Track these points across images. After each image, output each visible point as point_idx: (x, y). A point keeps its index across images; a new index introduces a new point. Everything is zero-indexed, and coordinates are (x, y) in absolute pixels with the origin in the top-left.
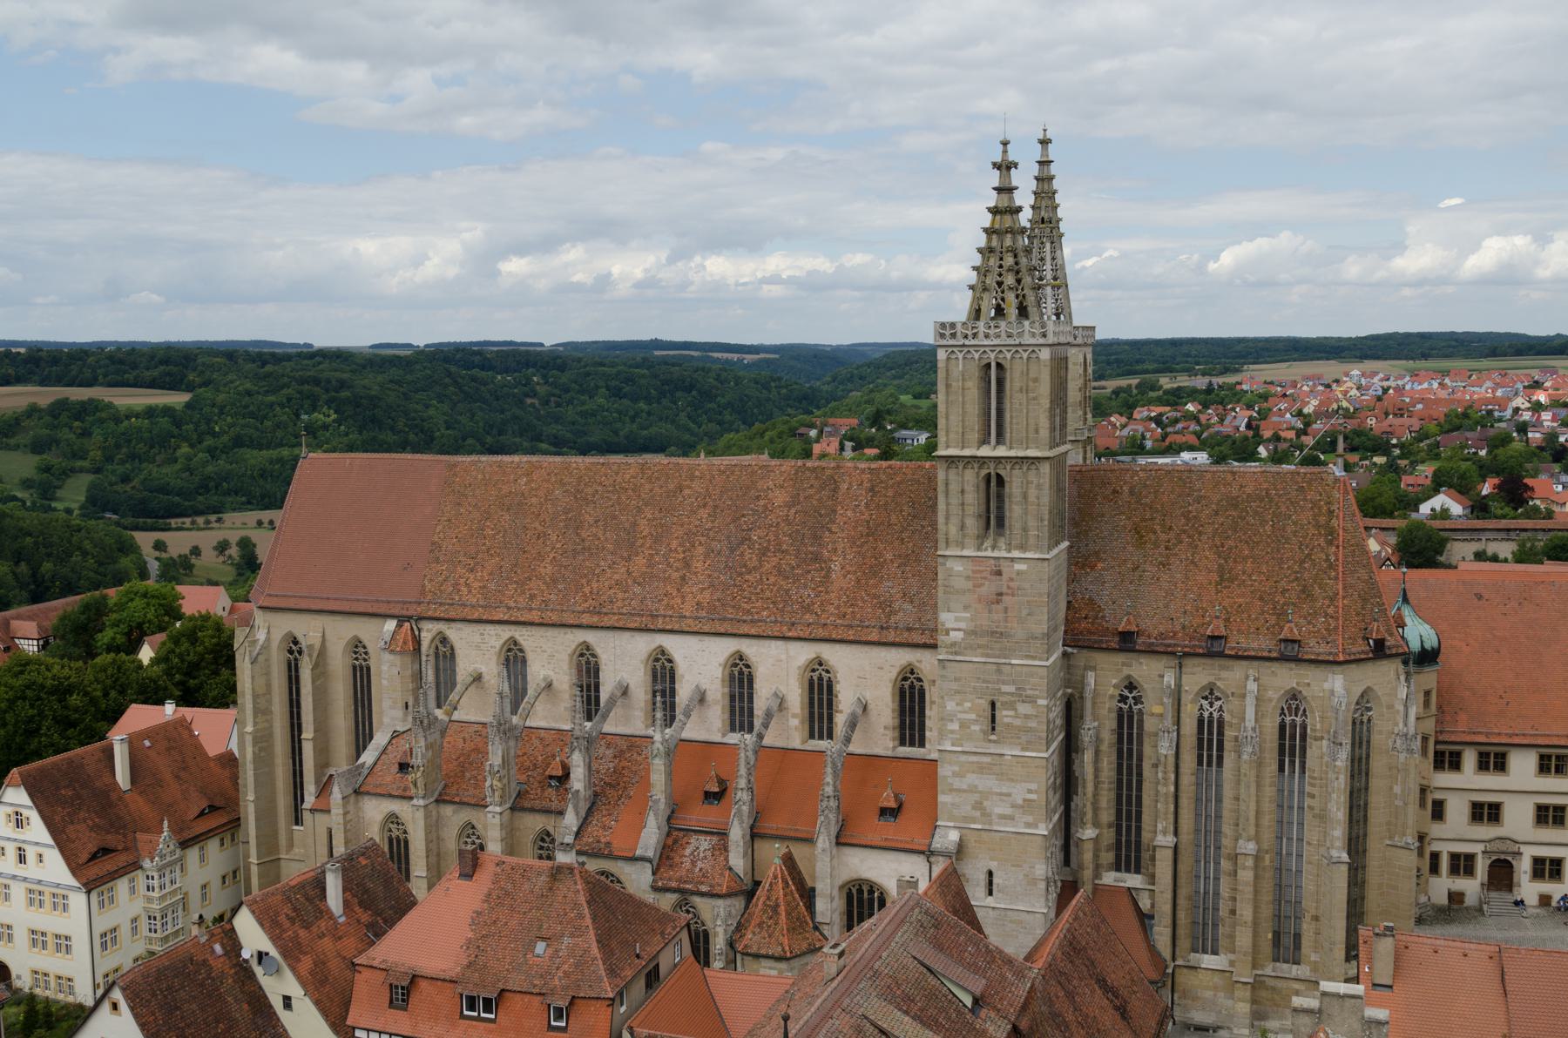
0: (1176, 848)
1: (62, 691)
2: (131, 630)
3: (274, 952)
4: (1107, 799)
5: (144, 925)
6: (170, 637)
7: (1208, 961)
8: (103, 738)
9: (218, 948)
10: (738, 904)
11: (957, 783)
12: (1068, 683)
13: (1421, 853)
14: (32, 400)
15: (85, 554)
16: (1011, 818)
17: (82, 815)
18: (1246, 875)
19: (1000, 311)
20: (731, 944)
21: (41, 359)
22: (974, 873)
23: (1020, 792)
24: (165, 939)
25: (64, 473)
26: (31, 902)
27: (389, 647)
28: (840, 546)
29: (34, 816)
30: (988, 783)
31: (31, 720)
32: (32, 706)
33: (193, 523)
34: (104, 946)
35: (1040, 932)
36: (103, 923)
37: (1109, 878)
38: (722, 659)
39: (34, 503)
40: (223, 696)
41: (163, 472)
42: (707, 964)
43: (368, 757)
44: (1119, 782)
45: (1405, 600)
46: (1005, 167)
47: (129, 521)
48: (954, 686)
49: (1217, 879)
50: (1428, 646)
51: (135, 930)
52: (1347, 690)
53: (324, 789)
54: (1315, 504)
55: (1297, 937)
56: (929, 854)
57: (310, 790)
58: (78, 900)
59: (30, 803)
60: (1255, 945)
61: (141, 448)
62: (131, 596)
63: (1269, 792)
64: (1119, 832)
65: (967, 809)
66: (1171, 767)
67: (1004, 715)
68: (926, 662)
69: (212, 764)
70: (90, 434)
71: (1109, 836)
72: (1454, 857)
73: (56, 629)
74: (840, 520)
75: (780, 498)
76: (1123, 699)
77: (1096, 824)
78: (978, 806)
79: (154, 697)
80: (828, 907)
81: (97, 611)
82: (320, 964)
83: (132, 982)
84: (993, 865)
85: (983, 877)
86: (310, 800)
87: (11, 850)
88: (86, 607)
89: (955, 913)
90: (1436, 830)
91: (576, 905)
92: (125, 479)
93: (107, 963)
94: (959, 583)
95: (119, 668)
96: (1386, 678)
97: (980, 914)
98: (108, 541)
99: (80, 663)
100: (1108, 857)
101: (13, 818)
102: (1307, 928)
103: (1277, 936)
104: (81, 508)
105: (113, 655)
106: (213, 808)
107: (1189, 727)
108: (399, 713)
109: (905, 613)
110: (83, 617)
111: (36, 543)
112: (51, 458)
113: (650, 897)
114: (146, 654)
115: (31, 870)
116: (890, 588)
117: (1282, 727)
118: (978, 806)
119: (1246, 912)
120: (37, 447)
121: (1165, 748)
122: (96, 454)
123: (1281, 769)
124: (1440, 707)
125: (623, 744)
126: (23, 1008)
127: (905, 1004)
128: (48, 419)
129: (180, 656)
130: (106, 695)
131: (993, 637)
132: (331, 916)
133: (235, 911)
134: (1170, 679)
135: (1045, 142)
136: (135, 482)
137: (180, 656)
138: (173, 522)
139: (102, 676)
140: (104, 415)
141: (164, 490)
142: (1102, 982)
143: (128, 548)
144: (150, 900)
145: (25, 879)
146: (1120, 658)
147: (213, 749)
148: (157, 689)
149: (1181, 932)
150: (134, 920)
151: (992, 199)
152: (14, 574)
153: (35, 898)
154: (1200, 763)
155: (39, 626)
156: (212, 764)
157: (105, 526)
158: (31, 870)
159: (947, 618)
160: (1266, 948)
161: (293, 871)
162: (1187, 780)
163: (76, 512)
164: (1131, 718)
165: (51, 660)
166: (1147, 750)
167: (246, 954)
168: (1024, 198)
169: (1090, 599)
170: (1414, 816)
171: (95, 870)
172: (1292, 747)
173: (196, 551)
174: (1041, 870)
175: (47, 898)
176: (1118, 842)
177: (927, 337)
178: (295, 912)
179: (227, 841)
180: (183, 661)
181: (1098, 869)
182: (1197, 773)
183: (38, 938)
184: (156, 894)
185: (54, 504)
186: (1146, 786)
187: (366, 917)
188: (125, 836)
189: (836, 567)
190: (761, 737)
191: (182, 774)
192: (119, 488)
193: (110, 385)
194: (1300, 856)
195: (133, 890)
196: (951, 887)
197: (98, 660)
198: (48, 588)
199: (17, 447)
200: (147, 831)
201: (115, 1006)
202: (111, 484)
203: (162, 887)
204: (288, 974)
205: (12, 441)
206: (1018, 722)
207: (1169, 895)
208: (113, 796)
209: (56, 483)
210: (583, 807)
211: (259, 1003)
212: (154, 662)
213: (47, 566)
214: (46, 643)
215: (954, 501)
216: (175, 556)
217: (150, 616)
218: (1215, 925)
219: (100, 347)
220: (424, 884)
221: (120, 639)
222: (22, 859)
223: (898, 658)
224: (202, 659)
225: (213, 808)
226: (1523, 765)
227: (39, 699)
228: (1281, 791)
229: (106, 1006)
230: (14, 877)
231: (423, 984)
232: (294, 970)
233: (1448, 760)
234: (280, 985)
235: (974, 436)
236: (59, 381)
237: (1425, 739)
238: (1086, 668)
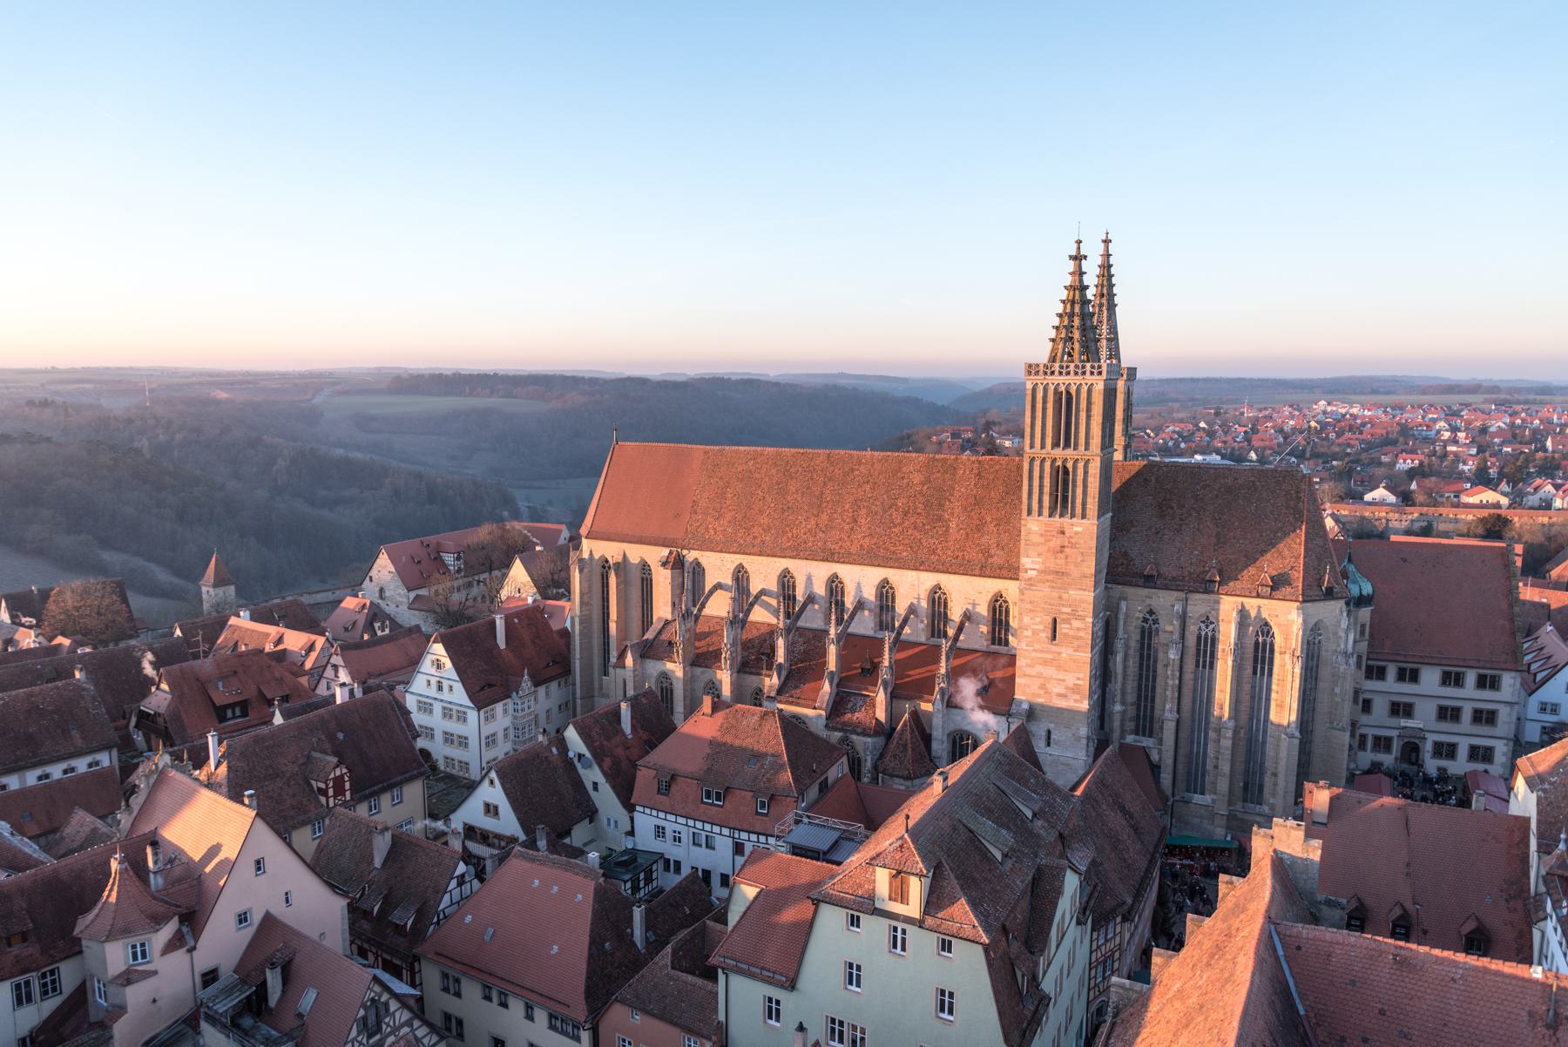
0: (1178, 722)
3: (588, 755)
4: (1131, 686)
7: (1197, 798)
9: (554, 750)
10: (880, 741)
11: (1029, 671)
12: (1106, 608)
13: (1353, 735)
16: (1064, 696)
18: (1227, 743)
19: (1070, 355)
20: (875, 767)
22: (1038, 729)
23: (1071, 680)
26: (445, 716)
27: (664, 564)
28: (956, 511)
30: (1049, 671)
34: (487, 744)
35: (1081, 772)
36: (487, 730)
37: (1130, 739)
38: (876, 582)
42: (859, 779)
43: (649, 635)
44: (1140, 676)
45: (1350, 560)
46: (1078, 258)
48: (1030, 607)
49: (1206, 744)
50: (1365, 593)
51: (506, 736)
52: (1304, 621)
53: (622, 656)
54: (1288, 493)
55: (1261, 787)
56: (1008, 714)
57: (614, 654)
58: (472, 715)
60: (1231, 790)
63: (1247, 687)
64: (1138, 708)
65: (1035, 688)
66: (1177, 668)
67: (1062, 628)
68: (1010, 589)
71: (1132, 712)
72: (1377, 739)
74: (957, 494)
75: (917, 478)
76: (1145, 620)
77: (1123, 703)
78: (1043, 686)
80: (940, 746)
82: (616, 762)
84: (1052, 726)
85: (1044, 734)
86: (613, 660)
87: (434, 681)
89: (1024, 756)
90: (1364, 719)
91: (776, 736)
93: (489, 755)
94: (1036, 539)
96: (1333, 611)
97: (1041, 758)
100: (1130, 725)
102: (1268, 779)
103: (1246, 785)
107: (1191, 640)
108: (669, 609)
109: (998, 558)
113: (824, 734)
116: (988, 540)
117: (1257, 643)
118: (1043, 686)
119: (1225, 768)
121: (1173, 655)
123: (1255, 673)
124: (1371, 635)
125: (810, 635)
127: (988, 812)
131: (1057, 576)
132: (623, 734)
134: (1178, 607)
135: (1107, 242)
142: (1123, 809)
146: (1146, 591)
149: (1180, 777)
151: (1068, 280)
153: (447, 714)
154: (1197, 666)
158: (446, 695)
159: (1026, 561)
160: (1239, 792)
161: (602, 704)
162: (1188, 677)
164: (1150, 633)
166: (1161, 655)
167: (571, 754)
168: (1091, 279)
169: (1126, 554)
170: (1347, 710)
172: (1263, 658)
173: (550, 502)
174: (1084, 731)
176: (1138, 716)
177: (1020, 374)
178: (601, 730)
181: (1123, 733)
182: (1195, 673)
183: (449, 738)
186: (1159, 679)
187: (645, 736)
189: (953, 525)
190: (899, 634)
194: (1265, 731)
195: (505, 711)
196: (1022, 739)
201: (492, 782)
204: (596, 768)
206: (1071, 633)
207: (1171, 753)
210: (784, 673)
211: (578, 784)
215: (1036, 483)
218: (1203, 776)
220: (682, 717)
222: (440, 688)
223: (991, 586)
226: (1430, 678)
228: (1253, 687)
229: (486, 782)
231: (680, 780)
232: (600, 767)
233: (1376, 673)
234: (592, 775)
235: (1049, 441)
237: (1359, 657)
238: (1121, 598)
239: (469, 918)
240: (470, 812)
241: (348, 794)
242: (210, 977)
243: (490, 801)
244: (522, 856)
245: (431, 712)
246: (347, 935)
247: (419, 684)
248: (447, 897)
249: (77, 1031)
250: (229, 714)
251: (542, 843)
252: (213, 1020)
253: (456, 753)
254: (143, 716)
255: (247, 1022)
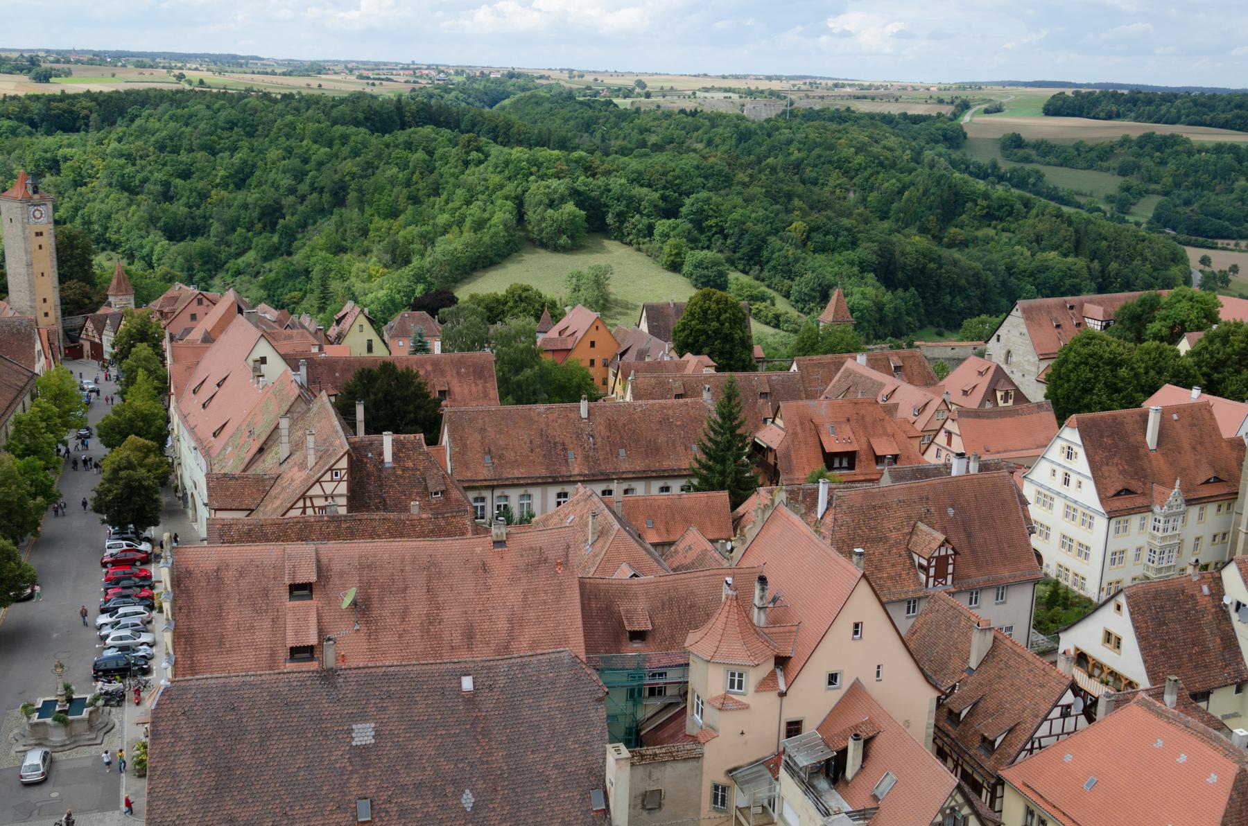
1: (1115, 363)
2: (1174, 326)
5: (1145, 554)
6: (1207, 336)
8: (1139, 406)
14: (1126, 132)
15: (1145, 259)
17: (1116, 460)
21: (1138, 99)
24: (1160, 570)
25: (1140, 193)
26: (1067, 514)
29: (1081, 453)
31: (1088, 381)
32: (1091, 371)
33: (1237, 245)
39: (1112, 215)
40: (1241, 392)
41: (1223, 201)
47: (1184, 237)
58: (1101, 523)
59: (1080, 442)
61: (1205, 178)
62: (1179, 298)
69: (1224, 444)
70: (1166, 163)
73: (1117, 315)
79: (1185, 382)
81: (1151, 306)
83: (1135, 594)
88: (1143, 302)
92: (1187, 203)
95: (1161, 354)
98: (1165, 252)
99: (1132, 345)
101: (1066, 450)
104: (1148, 223)
105: (1157, 342)
106: (1217, 480)
110: (1139, 309)
111: (1109, 246)
112: (1134, 181)
114: (1184, 346)
115: (1071, 491)
120: (1123, 171)
122: (1168, 180)
126: (1049, 588)
128: (1135, 148)
129: (1212, 354)
130: (1147, 373)
133: (1225, 565)
136: (1195, 206)
137: (1212, 354)
138: (1220, 242)
139: (1146, 357)
140: (1180, 148)
141: (1217, 215)
143: (1178, 259)
144: (1154, 537)
145: (1066, 497)
147: (1227, 433)
148: (1188, 376)
150: (1139, 549)
152: (1089, 268)
153: (1071, 511)
155: (1105, 311)
156: (1224, 444)
157: (1164, 239)
158: (1071, 491)
163: (1144, 226)
165: (1111, 339)
171: (1118, 504)
175: (1079, 515)
179: (1224, 508)
180: (1212, 357)
184: (1160, 534)
185: (1127, 217)
188: (1144, 484)
191: (1198, 447)
192: (1181, 209)
193: (1190, 124)
195: (1142, 526)
197: (1145, 345)
198: (1111, 283)
199: (1108, 169)
200: (1163, 484)
201: (1119, 608)
202: (1175, 206)
203: (1165, 530)
205: (1105, 164)
208: (1141, 452)
209: (1132, 200)
212: (1190, 354)
213: (1114, 266)
214: (1108, 325)
216: (1216, 271)
217: (1192, 317)
219: (1187, 92)
221: (1165, 331)
222: (1066, 482)
224: (1229, 358)
225: (1217, 480)
227: (1097, 366)
229: (1112, 606)
230: (1058, 494)
236: (1150, 118)
239: (1068, 758)
240: (1083, 636)
241: (950, 578)
242: (794, 728)
243: (1112, 630)
244: (1143, 703)
245: (1051, 507)
246: (931, 731)
247: (1041, 472)
248: (1046, 724)
249: (673, 737)
250: (836, 464)
251: (1170, 699)
252: (792, 770)
253: (1073, 563)
254: (757, 447)
255: (822, 784)
